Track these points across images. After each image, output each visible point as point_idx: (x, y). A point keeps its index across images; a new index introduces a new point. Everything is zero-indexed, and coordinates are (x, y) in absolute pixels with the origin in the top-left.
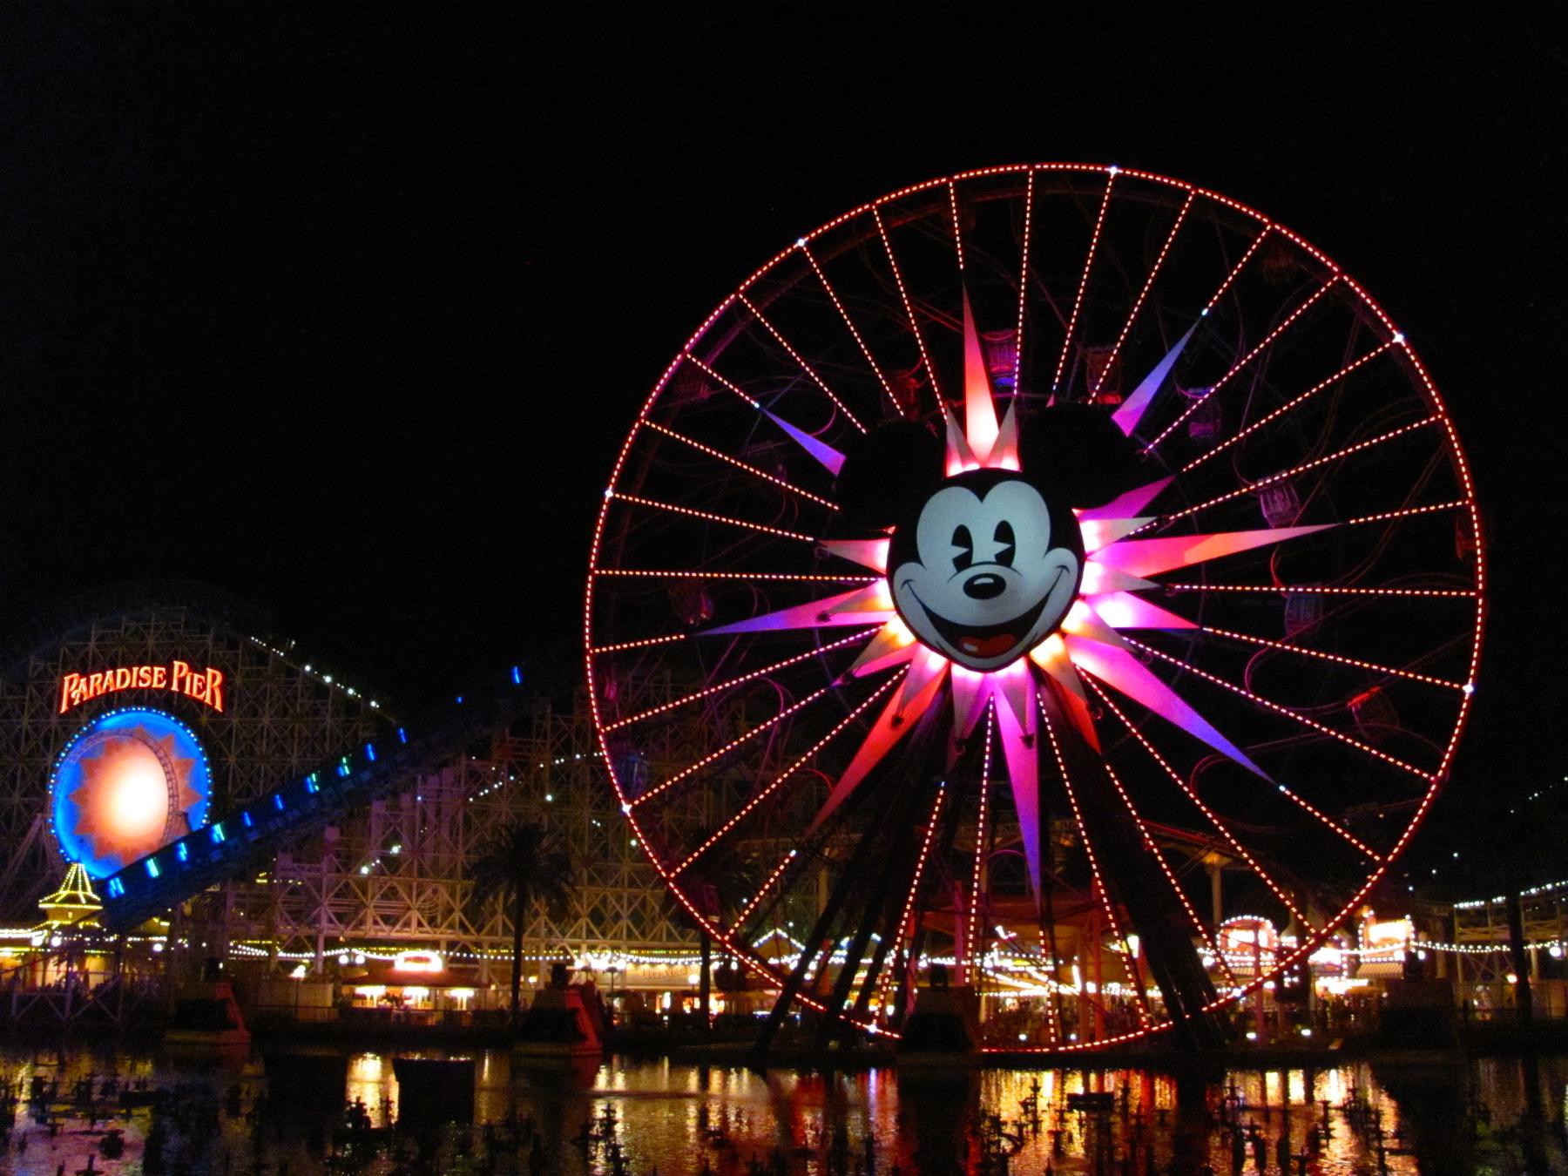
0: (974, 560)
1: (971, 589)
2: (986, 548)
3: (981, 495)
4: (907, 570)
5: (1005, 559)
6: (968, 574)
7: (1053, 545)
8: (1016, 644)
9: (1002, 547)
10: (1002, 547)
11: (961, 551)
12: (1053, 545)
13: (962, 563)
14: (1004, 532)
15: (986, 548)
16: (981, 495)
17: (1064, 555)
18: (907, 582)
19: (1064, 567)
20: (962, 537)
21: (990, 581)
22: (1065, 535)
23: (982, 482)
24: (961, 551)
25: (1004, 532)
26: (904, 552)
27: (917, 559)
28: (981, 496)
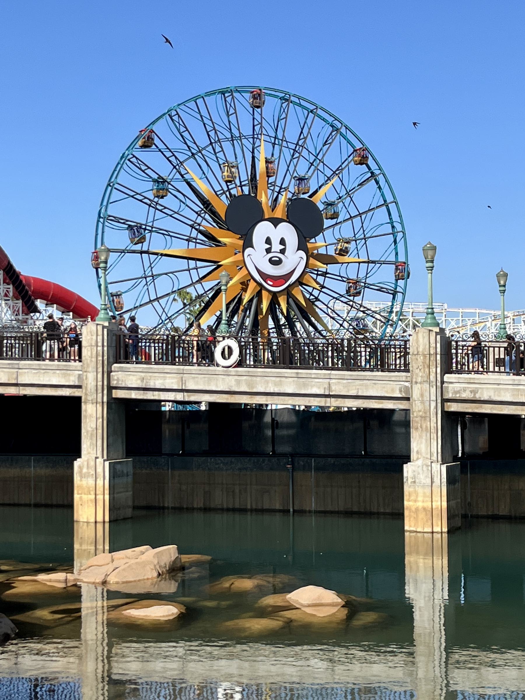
0: (272, 251)
1: (271, 261)
2: (276, 247)
3: (275, 227)
4: (248, 251)
5: (283, 252)
6: (270, 255)
7: (298, 249)
8: (286, 283)
9: (283, 247)
10: (283, 247)
11: (268, 246)
12: (298, 249)
13: (268, 251)
14: (282, 242)
15: (276, 247)
16: (275, 227)
17: (302, 254)
18: (249, 255)
19: (302, 258)
20: (268, 241)
21: (278, 259)
22: (302, 246)
23: (276, 222)
24: (268, 246)
25: (282, 242)
26: (248, 243)
27: (253, 247)
28: (275, 226)
